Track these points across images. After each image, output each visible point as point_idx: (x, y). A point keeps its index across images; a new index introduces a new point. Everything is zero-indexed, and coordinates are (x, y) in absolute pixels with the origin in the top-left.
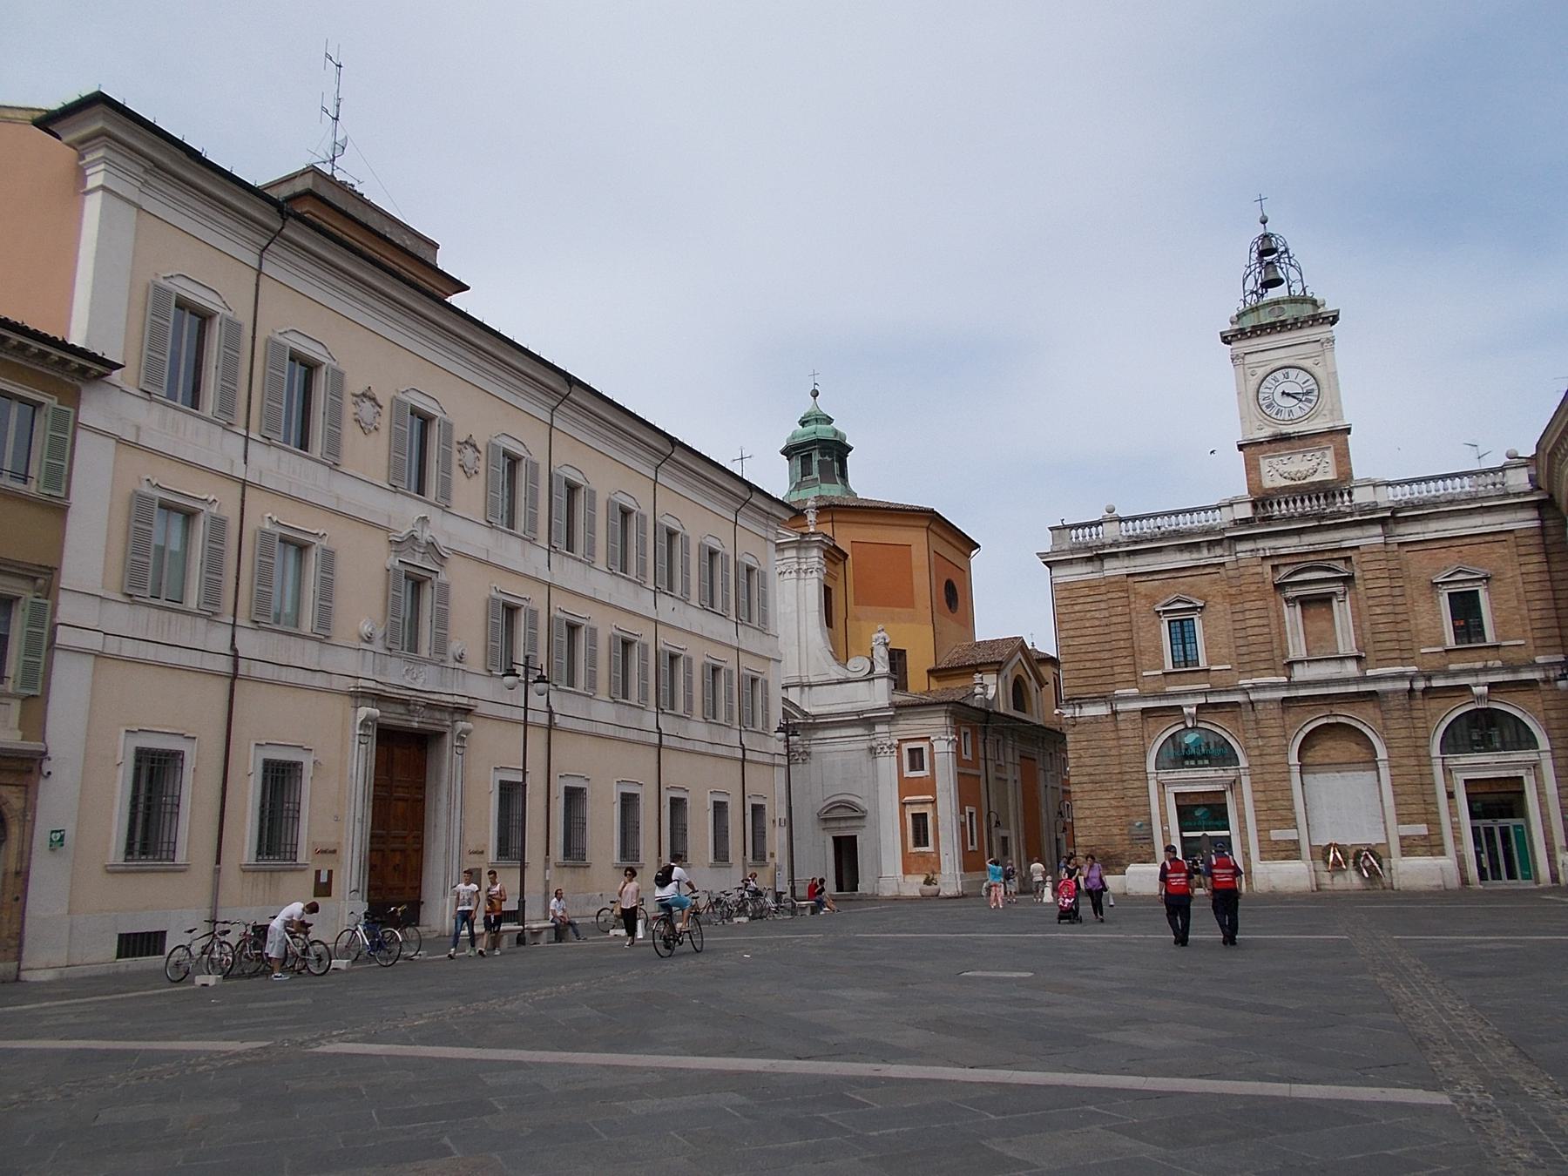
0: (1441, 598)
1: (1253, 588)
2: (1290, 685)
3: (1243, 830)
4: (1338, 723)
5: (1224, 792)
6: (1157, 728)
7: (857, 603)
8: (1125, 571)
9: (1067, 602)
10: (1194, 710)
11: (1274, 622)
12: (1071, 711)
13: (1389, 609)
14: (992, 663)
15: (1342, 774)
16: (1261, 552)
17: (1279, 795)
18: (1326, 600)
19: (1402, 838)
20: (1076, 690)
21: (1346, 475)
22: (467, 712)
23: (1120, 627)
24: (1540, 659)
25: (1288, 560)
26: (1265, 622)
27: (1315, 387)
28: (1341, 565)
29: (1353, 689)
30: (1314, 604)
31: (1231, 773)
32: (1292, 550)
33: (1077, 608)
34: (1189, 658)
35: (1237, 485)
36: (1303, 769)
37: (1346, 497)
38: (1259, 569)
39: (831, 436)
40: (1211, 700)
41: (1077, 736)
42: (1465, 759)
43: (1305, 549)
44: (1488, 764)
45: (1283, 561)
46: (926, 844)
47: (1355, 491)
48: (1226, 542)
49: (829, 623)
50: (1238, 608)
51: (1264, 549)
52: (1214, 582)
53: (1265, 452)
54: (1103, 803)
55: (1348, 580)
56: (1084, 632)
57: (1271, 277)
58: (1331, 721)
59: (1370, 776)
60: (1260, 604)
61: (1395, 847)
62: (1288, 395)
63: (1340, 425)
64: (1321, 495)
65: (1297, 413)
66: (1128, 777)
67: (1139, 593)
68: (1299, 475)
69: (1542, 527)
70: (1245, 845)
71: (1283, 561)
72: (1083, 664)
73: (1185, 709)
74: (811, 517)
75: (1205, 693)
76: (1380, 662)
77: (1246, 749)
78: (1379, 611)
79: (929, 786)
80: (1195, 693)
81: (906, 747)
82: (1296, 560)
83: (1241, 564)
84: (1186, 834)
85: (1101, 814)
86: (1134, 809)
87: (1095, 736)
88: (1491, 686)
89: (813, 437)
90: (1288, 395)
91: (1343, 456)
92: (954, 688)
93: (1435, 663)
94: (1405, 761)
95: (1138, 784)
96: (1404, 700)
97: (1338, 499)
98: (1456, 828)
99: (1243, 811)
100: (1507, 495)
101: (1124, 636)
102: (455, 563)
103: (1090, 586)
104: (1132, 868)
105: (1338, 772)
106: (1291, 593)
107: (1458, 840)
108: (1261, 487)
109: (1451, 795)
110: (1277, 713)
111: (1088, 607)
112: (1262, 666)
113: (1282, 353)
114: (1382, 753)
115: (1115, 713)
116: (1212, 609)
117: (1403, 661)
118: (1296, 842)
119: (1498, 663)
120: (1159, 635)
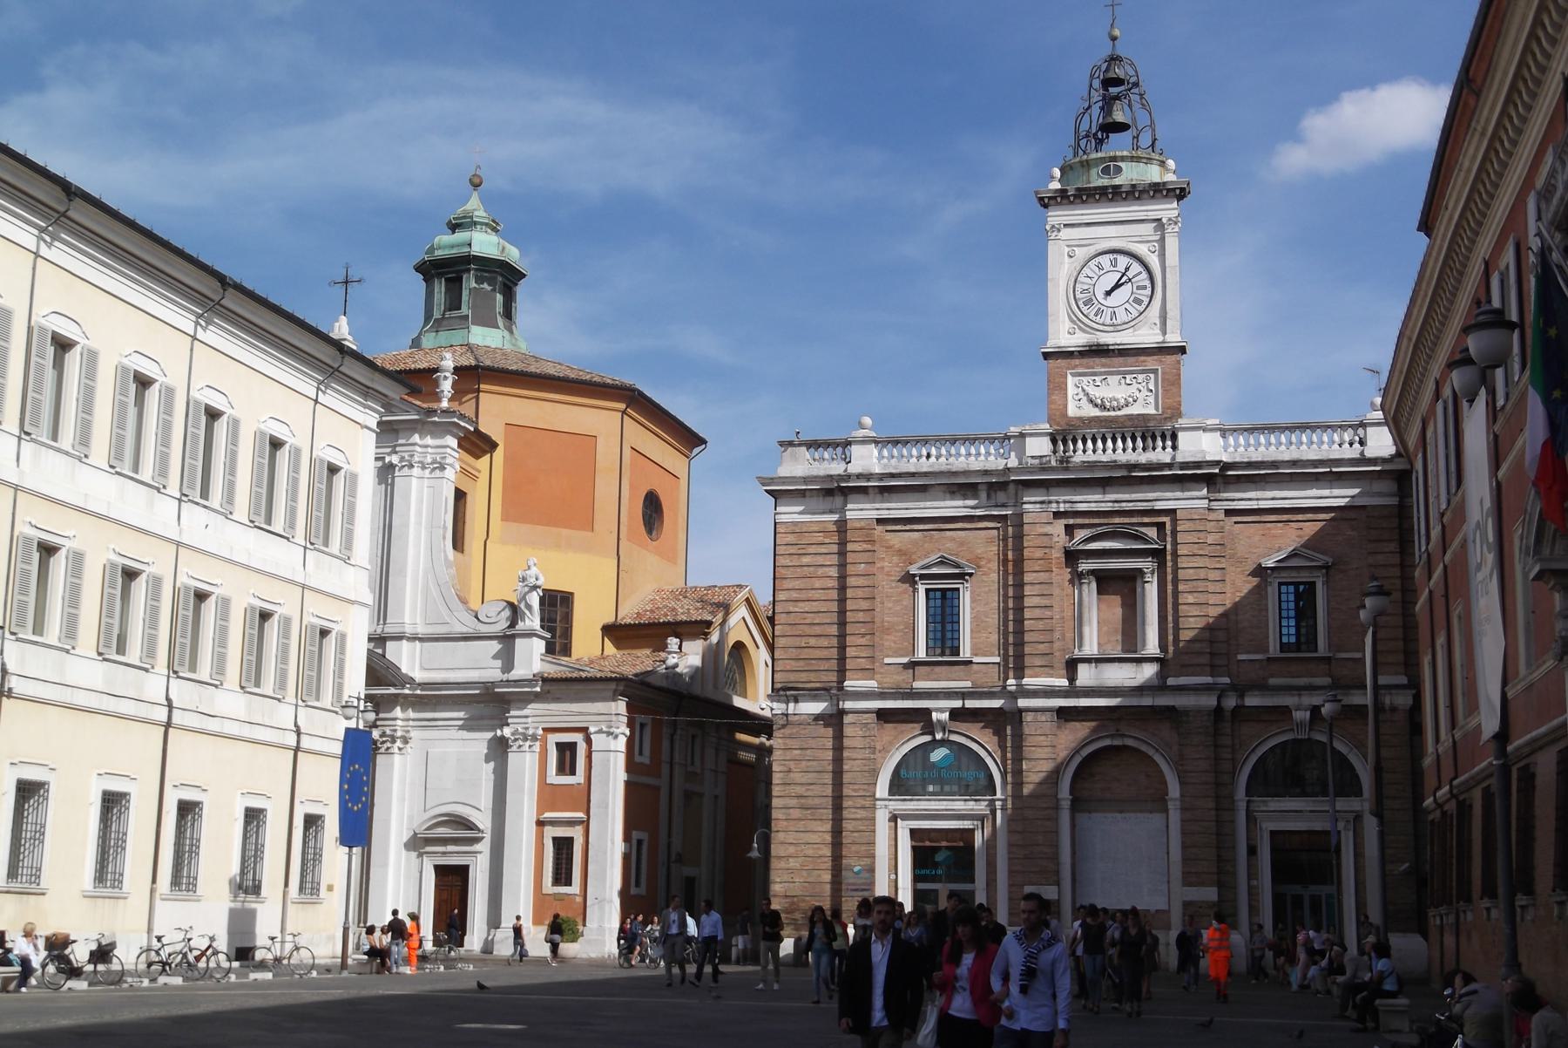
0: (1269, 589)
1: (1039, 553)
4: (1125, 747)
5: (973, 830)
6: (896, 737)
7: (506, 517)
8: (874, 514)
9: (793, 550)
10: (945, 716)
12: (783, 706)
13: (1202, 598)
14: (696, 622)
15: (1123, 815)
16: (1054, 505)
19: (1187, 905)
20: (792, 677)
23: (860, 593)
27: (1147, 283)
28: (1152, 533)
32: (1093, 507)
33: (806, 560)
34: (949, 644)
36: (1077, 804)
37: (1169, 443)
38: (1048, 529)
40: (970, 704)
41: (788, 741)
42: (1275, 804)
45: (1079, 521)
46: (569, 883)
47: (1181, 435)
48: (1012, 487)
49: (458, 543)
51: (1058, 502)
53: (1076, 366)
54: (814, 838)
55: (1158, 555)
56: (812, 594)
58: (1117, 742)
59: (1156, 820)
60: (1043, 577)
62: (1113, 289)
64: (1138, 435)
65: (1122, 316)
66: (850, 803)
67: (890, 547)
68: (1115, 404)
71: (1079, 521)
72: (804, 640)
73: (934, 715)
74: (446, 386)
75: (963, 695)
76: (1185, 669)
78: (1191, 599)
79: (583, 798)
84: (921, 886)
85: (810, 852)
86: (854, 848)
87: (812, 743)
90: (1113, 289)
91: (1172, 383)
92: (638, 661)
95: (862, 814)
97: (1159, 443)
98: (1253, 893)
100: (1363, 460)
101: (865, 605)
105: (1121, 812)
106: (1085, 566)
107: (1253, 909)
108: (1065, 414)
109: (1252, 851)
112: (1038, 661)
114: (1174, 790)
116: (985, 578)
117: (1214, 670)
119: (1327, 681)
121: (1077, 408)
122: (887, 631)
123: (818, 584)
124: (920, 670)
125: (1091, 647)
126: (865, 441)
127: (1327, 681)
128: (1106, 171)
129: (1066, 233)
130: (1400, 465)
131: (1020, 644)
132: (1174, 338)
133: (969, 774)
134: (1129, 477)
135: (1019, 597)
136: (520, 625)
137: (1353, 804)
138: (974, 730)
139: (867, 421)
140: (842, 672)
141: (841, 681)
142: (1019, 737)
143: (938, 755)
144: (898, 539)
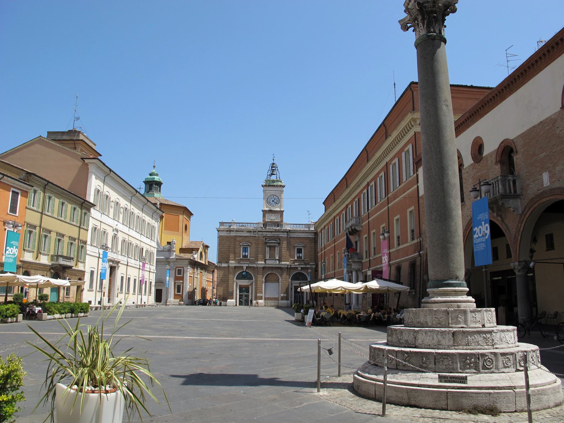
3: (252, 293)
7: (165, 229)
8: (235, 235)
11: (264, 250)
17: (260, 287)
18: (275, 247)
21: (282, 221)
22: (119, 262)
24: (310, 263)
25: (269, 237)
26: (262, 250)
29: (277, 266)
30: (272, 248)
31: (251, 281)
32: (269, 235)
33: (223, 242)
35: (261, 220)
39: (158, 180)
43: (272, 236)
45: (267, 237)
50: (257, 246)
52: (253, 240)
55: (279, 243)
57: (274, 173)
59: (278, 284)
60: (262, 246)
61: (280, 298)
63: (282, 210)
69: (315, 237)
70: (252, 296)
71: (267, 237)
77: (255, 277)
80: (246, 264)
81: (177, 269)
82: (270, 237)
83: (259, 237)
88: (302, 268)
89: (153, 180)
91: (282, 216)
94: (285, 282)
95: (232, 282)
98: (291, 295)
99: (252, 290)
101: (233, 249)
102: (119, 232)
103: (226, 237)
104: (228, 300)
107: (291, 297)
109: (291, 289)
110: (262, 269)
111: (225, 242)
112: (260, 259)
113: (273, 192)
115: (229, 266)
118: (262, 297)
119: (303, 263)
120: (240, 251)
122: (236, 254)
123: (225, 246)
124: (242, 260)
127: (303, 263)
128: (272, 182)
130: (315, 231)
134: (276, 231)
143: (244, 273)
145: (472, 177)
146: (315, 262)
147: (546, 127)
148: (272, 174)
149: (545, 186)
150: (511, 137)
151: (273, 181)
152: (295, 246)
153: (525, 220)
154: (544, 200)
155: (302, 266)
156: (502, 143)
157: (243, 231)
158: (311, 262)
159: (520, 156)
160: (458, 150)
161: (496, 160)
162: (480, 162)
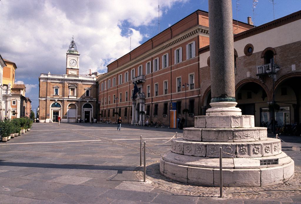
2: (69, 99)
8: (50, 81)
18: (74, 89)
19: (78, 117)
21: (78, 75)
28: (76, 85)
31: (60, 108)
44: (86, 109)
47: (79, 77)
55: (76, 87)
57: (73, 47)
59: (75, 110)
69: (96, 85)
75: (59, 98)
79: (16, 107)
88: (89, 101)
91: (78, 72)
93: (84, 98)
96: (80, 102)
98: (83, 117)
100: (94, 81)
106: (70, 88)
109: (83, 112)
114: (77, 107)
115: (47, 100)
121: (70, 73)
125: (70, 95)
126: (49, 74)
129: (69, 57)
131: (64, 94)
132: (78, 68)
133: (58, 105)
135: (64, 90)
136: (8, 89)
137: (91, 109)
138: (60, 102)
139: (49, 72)
140: (47, 96)
141: (47, 97)
142: (64, 103)
144: (52, 84)
145: (244, 62)
146: (96, 98)
147: (296, 45)
148: (72, 47)
149: (292, 70)
150: (273, 46)
151: (73, 51)
152: (85, 89)
153: (278, 84)
154: (292, 76)
155: (89, 100)
156: (267, 48)
157: (55, 79)
158: (94, 98)
159: (278, 56)
160: (234, 49)
161: (262, 56)
162: (250, 56)
